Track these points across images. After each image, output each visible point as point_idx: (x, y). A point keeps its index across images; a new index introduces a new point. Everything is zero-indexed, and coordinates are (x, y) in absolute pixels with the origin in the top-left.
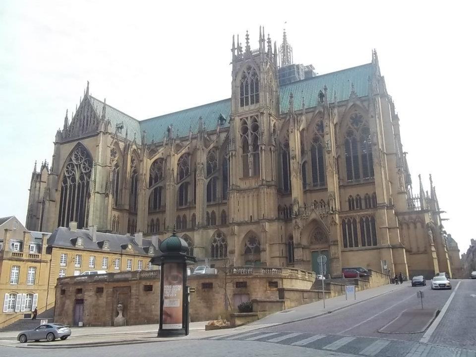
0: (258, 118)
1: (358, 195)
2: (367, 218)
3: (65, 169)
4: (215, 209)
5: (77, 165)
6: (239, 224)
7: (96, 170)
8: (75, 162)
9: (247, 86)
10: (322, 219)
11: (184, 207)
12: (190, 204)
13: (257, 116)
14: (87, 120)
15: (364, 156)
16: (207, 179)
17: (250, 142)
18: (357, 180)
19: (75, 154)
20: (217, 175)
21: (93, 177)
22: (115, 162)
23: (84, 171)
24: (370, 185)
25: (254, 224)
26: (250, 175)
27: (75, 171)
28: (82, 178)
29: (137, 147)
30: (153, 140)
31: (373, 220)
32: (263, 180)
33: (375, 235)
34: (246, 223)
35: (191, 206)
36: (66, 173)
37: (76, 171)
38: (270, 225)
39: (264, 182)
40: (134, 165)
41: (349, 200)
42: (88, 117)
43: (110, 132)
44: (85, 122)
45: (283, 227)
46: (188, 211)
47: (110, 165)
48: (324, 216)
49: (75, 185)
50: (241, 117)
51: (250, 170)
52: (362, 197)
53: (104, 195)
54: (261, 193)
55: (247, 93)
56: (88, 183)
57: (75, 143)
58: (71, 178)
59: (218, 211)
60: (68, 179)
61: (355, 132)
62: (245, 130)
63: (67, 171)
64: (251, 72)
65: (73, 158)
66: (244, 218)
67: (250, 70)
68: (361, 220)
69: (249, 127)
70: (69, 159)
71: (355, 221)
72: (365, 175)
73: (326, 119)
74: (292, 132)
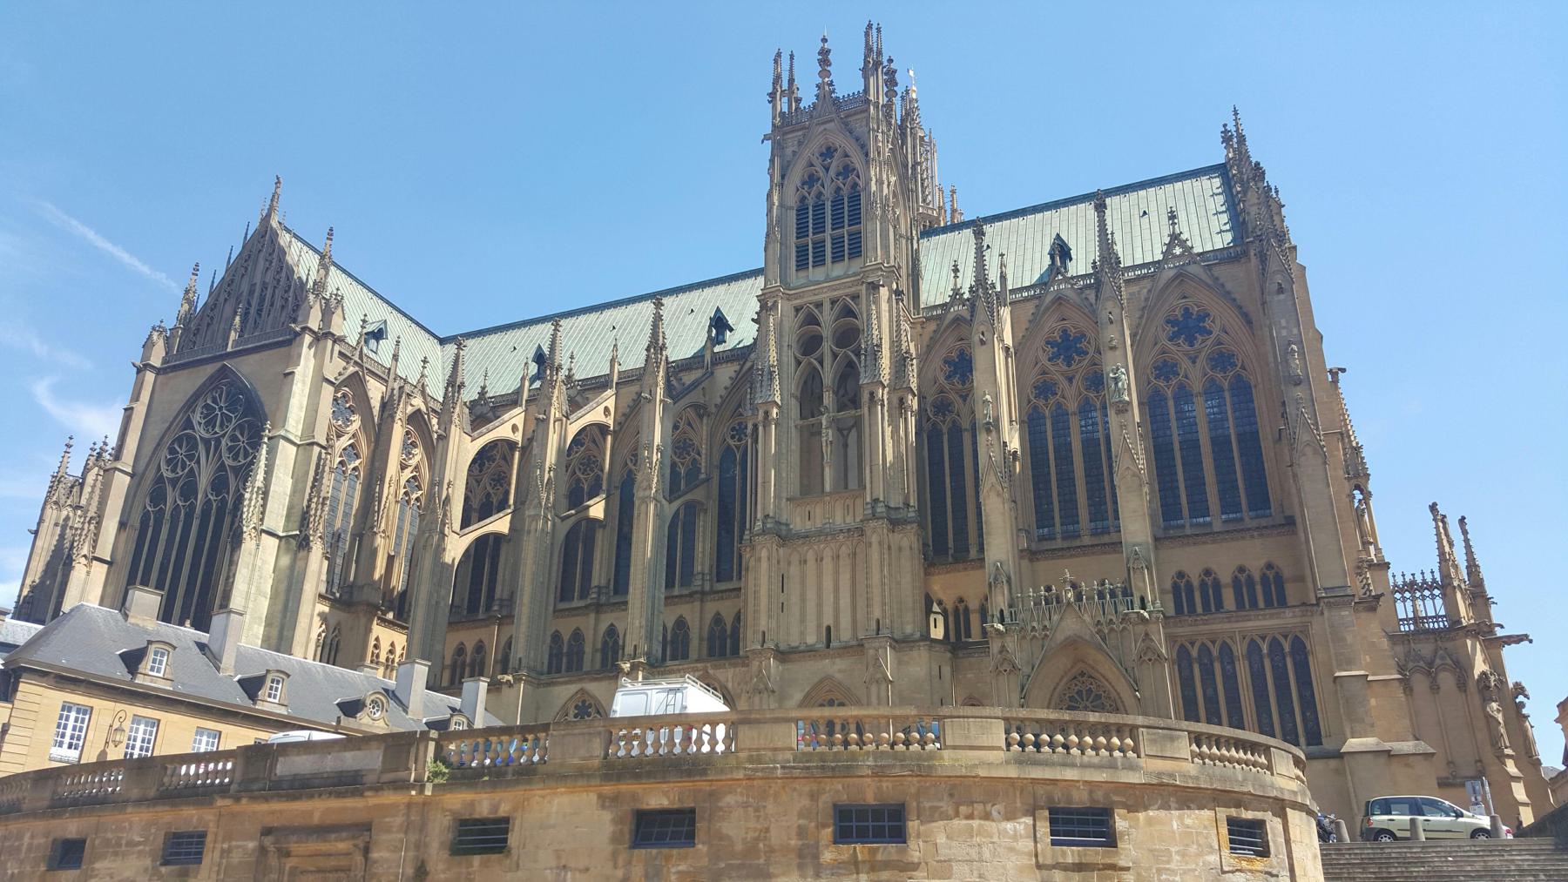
0: (857, 305)
1: (1208, 572)
2: (1275, 646)
3: (164, 454)
4: (689, 612)
5: (207, 442)
6: (783, 655)
7: (272, 453)
8: (201, 432)
9: (819, 207)
10: (1104, 639)
11: (576, 603)
12: (599, 594)
13: (855, 297)
14: (262, 299)
15: (1221, 445)
16: (670, 502)
17: (828, 375)
18: (1201, 520)
19: (207, 406)
20: (698, 495)
21: (260, 476)
22: (345, 442)
23: (229, 462)
24: (1252, 537)
25: (840, 656)
26: (828, 488)
27: (198, 462)
28: (219, 484)
29: (426, 403)
30: (483, 388)
31: (1300, 651)
32: (876, 501)
33: (1309, 703)
34: (810, 652)
35: (603, 599)
36: (163, 467)
37: (203, 460)
38: (900, 663)
39: (880, 509)
40: (413, 462)
41: (1176, 588)
42: (265, 286)
43: (338, 333)
44: (254, 303)
45: (946, 670)
46: (592, 616)
47: (324, 443)
48: (1112, 630)
49: (192, 507)
50: (798, 302)
51: (827, 471)
52: (1225, 577)
53: (294, 543)
54: (871, 543)
55: (819, 227)
56: (239, 499)
57: (210, 369)
58: (180, 484)
59: (696, 616)
60: (169, 489)
61: (1185, 364)
62: (810, 344)
63: (169, 462)
64: (835, 164)
65: (197, 418)
66: (802, 633)
67: (832, 157)
68: (1253, 648)
69: (824, 334)
70: (181, 419)
71: (1226, 650)
72: (1230, 504)
73: (1107, 299)
74: (983, 342)
